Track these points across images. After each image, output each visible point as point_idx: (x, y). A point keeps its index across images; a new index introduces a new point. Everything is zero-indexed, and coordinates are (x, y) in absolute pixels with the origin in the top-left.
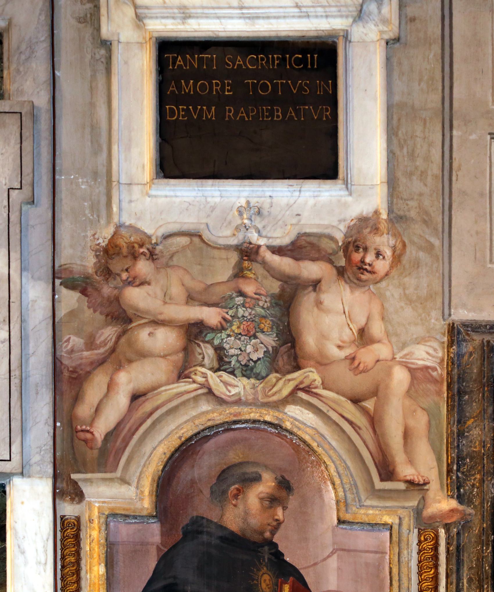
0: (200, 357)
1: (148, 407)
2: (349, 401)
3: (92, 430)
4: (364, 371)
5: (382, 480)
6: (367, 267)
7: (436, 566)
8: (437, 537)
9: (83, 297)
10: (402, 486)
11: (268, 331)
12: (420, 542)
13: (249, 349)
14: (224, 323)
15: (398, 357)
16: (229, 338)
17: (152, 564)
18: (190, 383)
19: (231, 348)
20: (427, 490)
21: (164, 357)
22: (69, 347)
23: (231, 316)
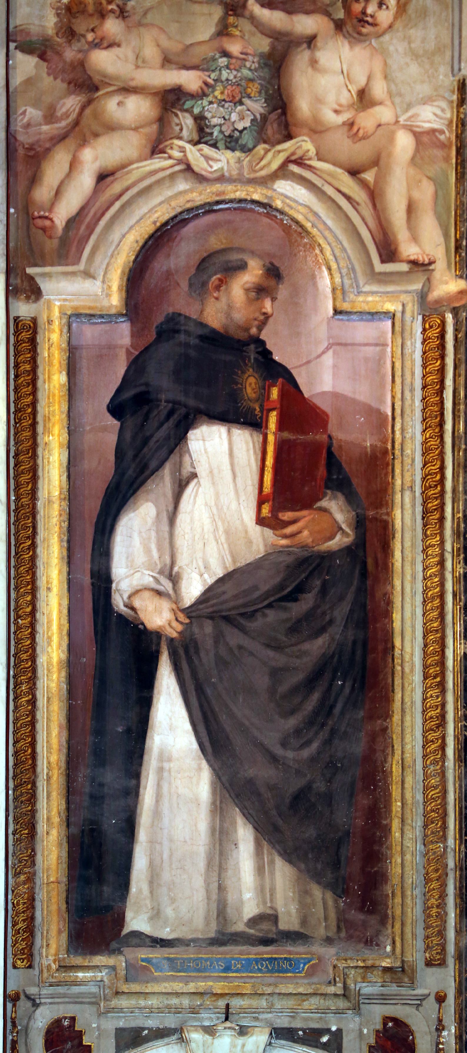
0: (177, 128)
1: (117, 188)
2: (346, 174)
3: (51, 216)
4: (364, 138)
5: (383, 261)
6: (369, 19)
7: (443, 357)
8: (443, 324)
9: (41, 62)
10: (404, 267)
11: (255, 97)
12: (424, 330)
13: (234, 117)
14: (205, 88)
15: (402, 120)
16: (211, 106)
17: (121, 368)
18: (165, 159)
19: (213, 117)
20: (433, 270)
21: (136, 129)
22: (25, 120)
23: (214, 80)
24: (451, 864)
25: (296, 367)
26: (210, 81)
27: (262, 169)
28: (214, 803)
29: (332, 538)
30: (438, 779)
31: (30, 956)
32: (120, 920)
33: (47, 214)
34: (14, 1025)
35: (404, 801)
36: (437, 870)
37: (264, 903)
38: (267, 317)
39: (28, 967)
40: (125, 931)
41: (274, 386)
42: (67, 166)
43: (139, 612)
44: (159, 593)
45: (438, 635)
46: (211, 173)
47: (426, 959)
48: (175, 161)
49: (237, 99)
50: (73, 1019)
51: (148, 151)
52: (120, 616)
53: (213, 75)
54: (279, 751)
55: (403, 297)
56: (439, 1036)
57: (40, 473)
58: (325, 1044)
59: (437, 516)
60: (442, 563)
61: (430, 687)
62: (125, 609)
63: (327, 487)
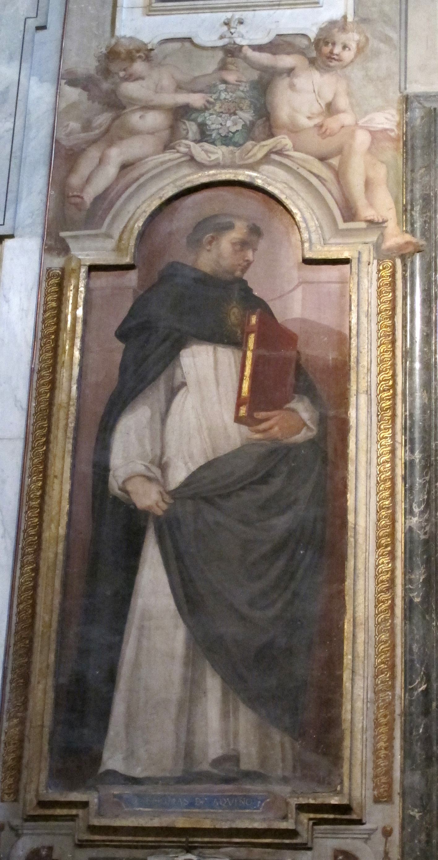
0: (184, 132)
1: (135, 174)
2: (317, 160)
4: (331, 135)
6: (335, 57)
7: (394, 291)
8: (394, 266)
10: (363, 225)
11: (246, 109)
12: (379, 271)
13: (229, 123)
15: (360, 123)
17: (129, 305)
18: (174, 153)
19: (213, 124)
20: (386, 227)
21: (152, 133)
23: (214, 99)
24: (398, 710)
25: (272, 300)
26: (212, 100)
27: (249, 158)
28: (187, 656)
29: (298, 432)
30: (388, 635)
31: (16, 792)
32: (97, 759)
33: (79, 194)
35: (356, 654)
36: (385, 716)
37: (228, 745)
38: (249, 263)
39: (13, 801)
40: (102, 769)
41: (254, 314)
42: (97, 160)
43: (131, 495)
44: (149, 479)
45: (390, 511)
46: (210, 161)
47: (374, 796)
48: (182, 155)
49: (232, 111)
51: (161, 147)
52: (115, 498)
53: (214, 96)
54: (245, 610)
55: (360, 247)
57: (58, 384)
59: (390, 414)
60: (393, 452)
61: (382, 555)
62: (119, 492)
63: (295, 392)
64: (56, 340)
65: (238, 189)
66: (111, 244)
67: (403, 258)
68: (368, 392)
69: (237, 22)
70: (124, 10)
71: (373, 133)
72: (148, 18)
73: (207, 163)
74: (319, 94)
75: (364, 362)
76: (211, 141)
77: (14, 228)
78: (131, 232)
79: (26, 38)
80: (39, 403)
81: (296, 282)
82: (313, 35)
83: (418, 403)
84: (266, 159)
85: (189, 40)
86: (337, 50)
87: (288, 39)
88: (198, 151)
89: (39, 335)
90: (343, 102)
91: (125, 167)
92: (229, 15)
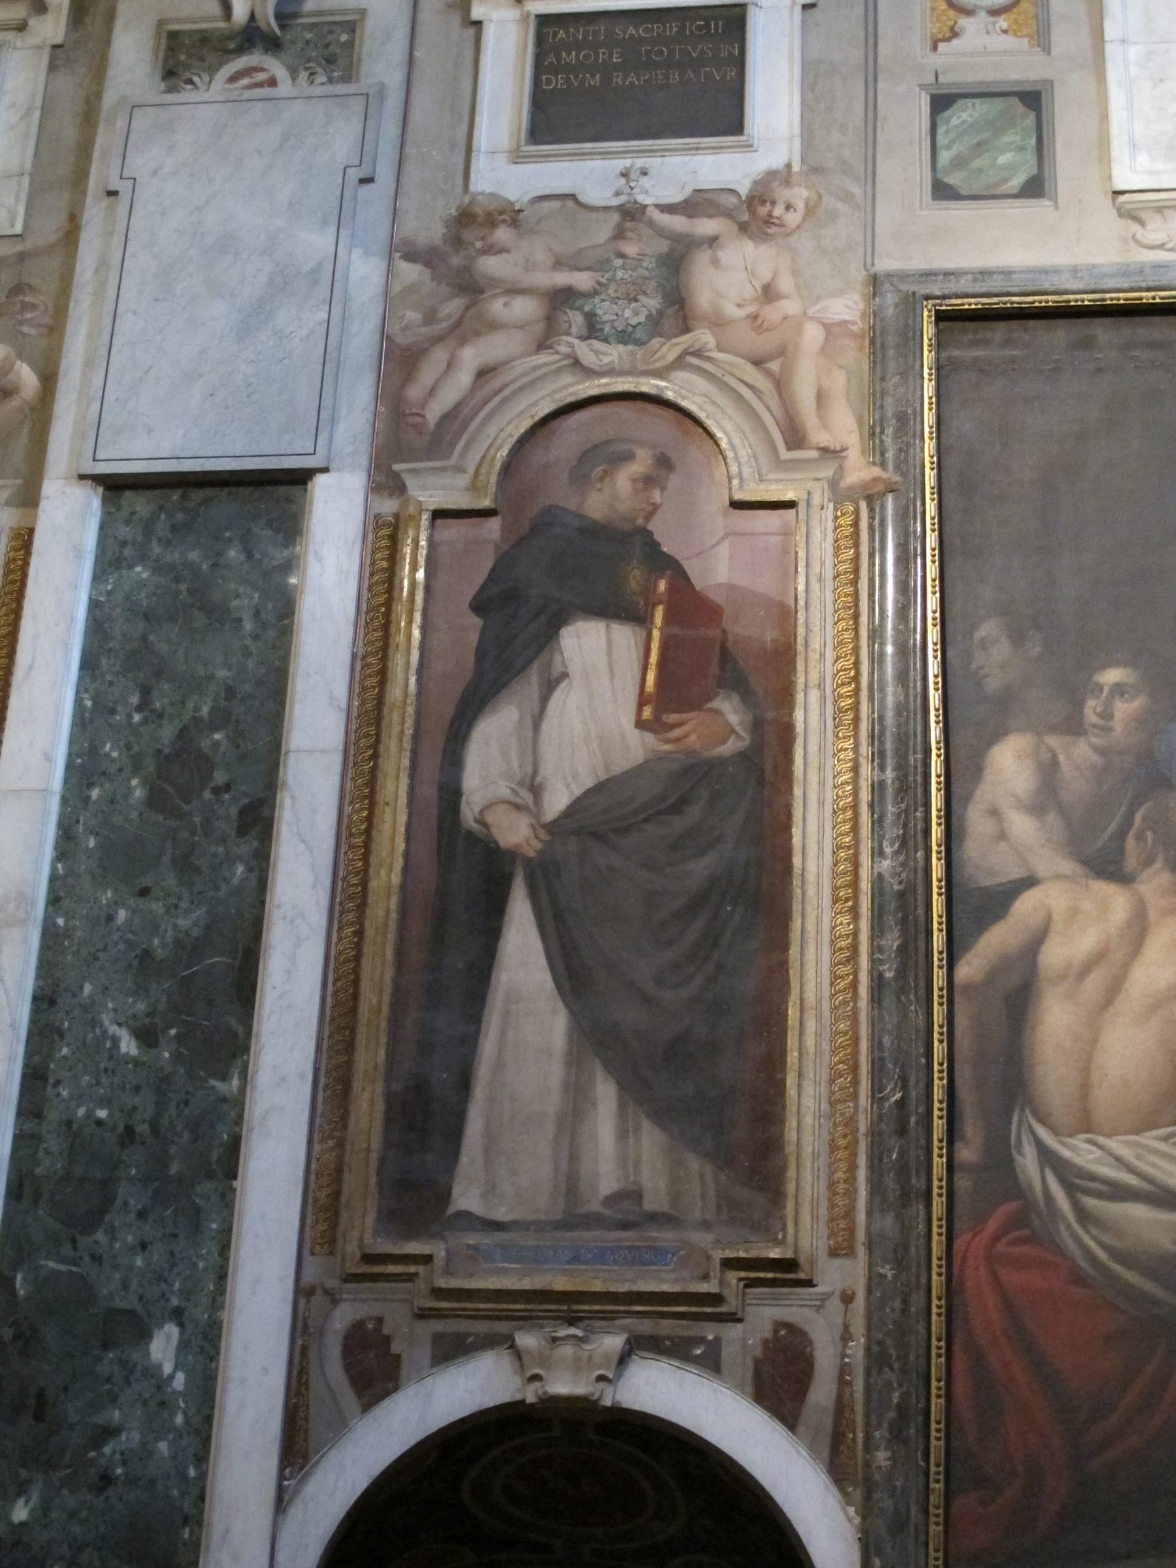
0: (566, 325)
1: (497, 383)
2: (749, 365)
3: (423, 413)
4: (768, 330)
5: (789, 448)
6: (775, 221)
7: (857, 545)
8: (857, 512)
10: (814, 454)
12: (836, 518)
13: (628, 313)
15: (810, 312)
17: (487, 564)
18: (552, 354)
19: (605, 314)
20: (846, 457)
21: (521, 327)
23: (608, 280)
24: (863, 1128)
25: (687, 558)
26: (604, 280)
27: (655, 361)
28: (569, 1053)
29: (724, 742)
30: (848, 1023)
31: (332, 1241)
32: (445, 1197)
33: (419, 411)
34: (306, 1326)
35: (804, 1050)
36: (845, 1136)
37: (627, 1176)
38: (655, 508)
39: (327, 1254)
40: (451, 1210)
42: (444, 364)
43: (492, 829)
44: (517, 807)
45: (851, 852)
46: (601, 366)
47: (830, 1247)
49: (632, 296)
50: (379, 1320)
52: (470, 834)
53: (607, 275)
55: (810, 485)
56: (845, 1346)
57: (389, 676)
58: (698, 1356)
59: (851, 716)
60: (855, 769)
61: (840, 913)
62: (475, 825)
63: (720, 686)
64: (388, 615)
65: (640, 405)
66: (464, 480)
67: (869, 499)
68: (821, 687)
69: (638, 172)
70: (482, 156)
71: (828, 327)
72: (514, 166)
73: (597, 368)
74: (752, 273)
75: (815, 644)
76: (603, 337)
77: (329, 459)
78: (492, 464)
79: (346, 194)
80: (363, 702)
81: (721, 533)
82: (744, 191)
83: (890, 701)
84: (679, 363)
85: (573, 197)
86: (778, 211)
87: (710, 196)
88: (586, 352)
89: (364, 607)
90: (785, 284)
91: (483, 373)
92: (627, 162)
